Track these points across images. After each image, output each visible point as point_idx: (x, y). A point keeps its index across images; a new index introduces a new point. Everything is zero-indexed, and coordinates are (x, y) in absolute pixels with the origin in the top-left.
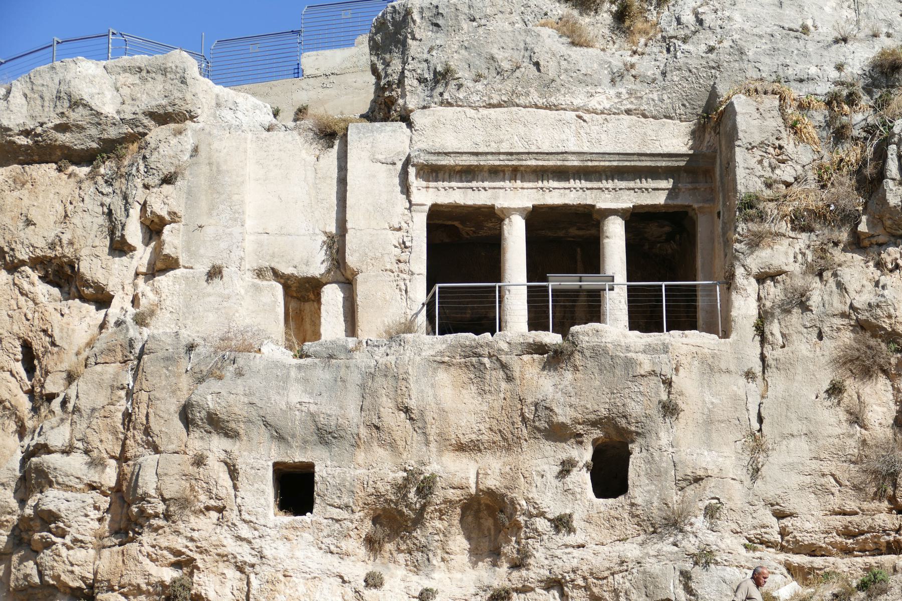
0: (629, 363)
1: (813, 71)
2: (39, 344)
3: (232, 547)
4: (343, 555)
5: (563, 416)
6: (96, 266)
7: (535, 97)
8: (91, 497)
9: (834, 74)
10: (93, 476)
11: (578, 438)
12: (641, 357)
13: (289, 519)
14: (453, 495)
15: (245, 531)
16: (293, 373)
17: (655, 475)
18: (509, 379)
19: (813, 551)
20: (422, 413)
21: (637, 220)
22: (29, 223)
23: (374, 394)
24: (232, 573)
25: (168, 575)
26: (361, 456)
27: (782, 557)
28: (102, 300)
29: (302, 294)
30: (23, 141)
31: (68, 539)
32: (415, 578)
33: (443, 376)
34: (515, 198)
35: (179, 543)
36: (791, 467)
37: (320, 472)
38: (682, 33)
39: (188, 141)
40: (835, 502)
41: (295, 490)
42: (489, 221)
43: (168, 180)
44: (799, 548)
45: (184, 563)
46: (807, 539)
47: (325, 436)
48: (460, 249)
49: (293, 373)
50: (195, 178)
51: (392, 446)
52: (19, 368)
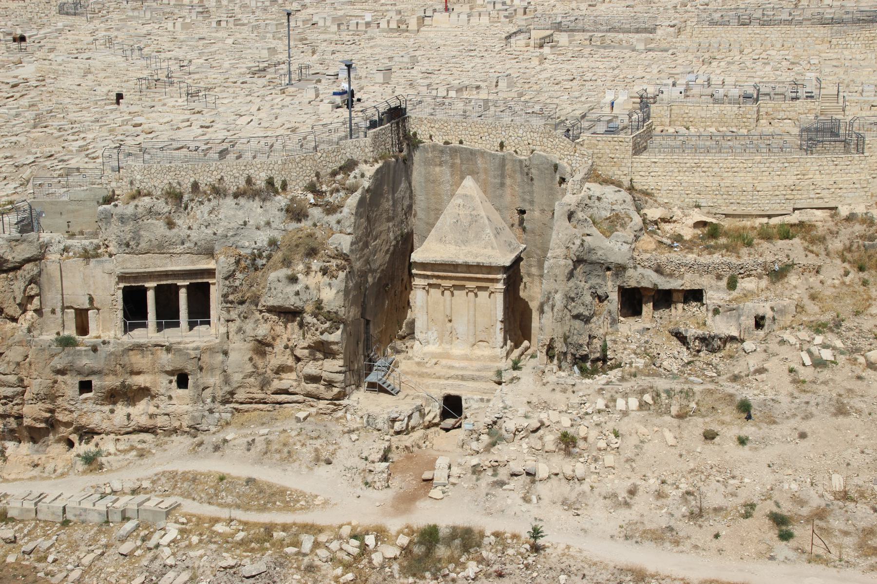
0: (188, 354)
3: (69, 407)
4: (102, 405)
5: (169, 368)
7: (157, 251)
8: (20, 389)
9: (254, 246)
11: (173, 375)
12: (192, 352)
13: (85, 396)
14: (135, 388)
17: (196, 386)
19: (242, 403)
23: (110, 360)
25: (48, 415)
26: (107, 378)
27: (232, 405)
28: (14, 320)
32: (124, 408)
33: (131, 353)
35: (51, 406)
40: (248, 390)
41: (85, 387)
44: (237, 402)
45: (52, 411)
47: (93, 373)
50: (43, 279)
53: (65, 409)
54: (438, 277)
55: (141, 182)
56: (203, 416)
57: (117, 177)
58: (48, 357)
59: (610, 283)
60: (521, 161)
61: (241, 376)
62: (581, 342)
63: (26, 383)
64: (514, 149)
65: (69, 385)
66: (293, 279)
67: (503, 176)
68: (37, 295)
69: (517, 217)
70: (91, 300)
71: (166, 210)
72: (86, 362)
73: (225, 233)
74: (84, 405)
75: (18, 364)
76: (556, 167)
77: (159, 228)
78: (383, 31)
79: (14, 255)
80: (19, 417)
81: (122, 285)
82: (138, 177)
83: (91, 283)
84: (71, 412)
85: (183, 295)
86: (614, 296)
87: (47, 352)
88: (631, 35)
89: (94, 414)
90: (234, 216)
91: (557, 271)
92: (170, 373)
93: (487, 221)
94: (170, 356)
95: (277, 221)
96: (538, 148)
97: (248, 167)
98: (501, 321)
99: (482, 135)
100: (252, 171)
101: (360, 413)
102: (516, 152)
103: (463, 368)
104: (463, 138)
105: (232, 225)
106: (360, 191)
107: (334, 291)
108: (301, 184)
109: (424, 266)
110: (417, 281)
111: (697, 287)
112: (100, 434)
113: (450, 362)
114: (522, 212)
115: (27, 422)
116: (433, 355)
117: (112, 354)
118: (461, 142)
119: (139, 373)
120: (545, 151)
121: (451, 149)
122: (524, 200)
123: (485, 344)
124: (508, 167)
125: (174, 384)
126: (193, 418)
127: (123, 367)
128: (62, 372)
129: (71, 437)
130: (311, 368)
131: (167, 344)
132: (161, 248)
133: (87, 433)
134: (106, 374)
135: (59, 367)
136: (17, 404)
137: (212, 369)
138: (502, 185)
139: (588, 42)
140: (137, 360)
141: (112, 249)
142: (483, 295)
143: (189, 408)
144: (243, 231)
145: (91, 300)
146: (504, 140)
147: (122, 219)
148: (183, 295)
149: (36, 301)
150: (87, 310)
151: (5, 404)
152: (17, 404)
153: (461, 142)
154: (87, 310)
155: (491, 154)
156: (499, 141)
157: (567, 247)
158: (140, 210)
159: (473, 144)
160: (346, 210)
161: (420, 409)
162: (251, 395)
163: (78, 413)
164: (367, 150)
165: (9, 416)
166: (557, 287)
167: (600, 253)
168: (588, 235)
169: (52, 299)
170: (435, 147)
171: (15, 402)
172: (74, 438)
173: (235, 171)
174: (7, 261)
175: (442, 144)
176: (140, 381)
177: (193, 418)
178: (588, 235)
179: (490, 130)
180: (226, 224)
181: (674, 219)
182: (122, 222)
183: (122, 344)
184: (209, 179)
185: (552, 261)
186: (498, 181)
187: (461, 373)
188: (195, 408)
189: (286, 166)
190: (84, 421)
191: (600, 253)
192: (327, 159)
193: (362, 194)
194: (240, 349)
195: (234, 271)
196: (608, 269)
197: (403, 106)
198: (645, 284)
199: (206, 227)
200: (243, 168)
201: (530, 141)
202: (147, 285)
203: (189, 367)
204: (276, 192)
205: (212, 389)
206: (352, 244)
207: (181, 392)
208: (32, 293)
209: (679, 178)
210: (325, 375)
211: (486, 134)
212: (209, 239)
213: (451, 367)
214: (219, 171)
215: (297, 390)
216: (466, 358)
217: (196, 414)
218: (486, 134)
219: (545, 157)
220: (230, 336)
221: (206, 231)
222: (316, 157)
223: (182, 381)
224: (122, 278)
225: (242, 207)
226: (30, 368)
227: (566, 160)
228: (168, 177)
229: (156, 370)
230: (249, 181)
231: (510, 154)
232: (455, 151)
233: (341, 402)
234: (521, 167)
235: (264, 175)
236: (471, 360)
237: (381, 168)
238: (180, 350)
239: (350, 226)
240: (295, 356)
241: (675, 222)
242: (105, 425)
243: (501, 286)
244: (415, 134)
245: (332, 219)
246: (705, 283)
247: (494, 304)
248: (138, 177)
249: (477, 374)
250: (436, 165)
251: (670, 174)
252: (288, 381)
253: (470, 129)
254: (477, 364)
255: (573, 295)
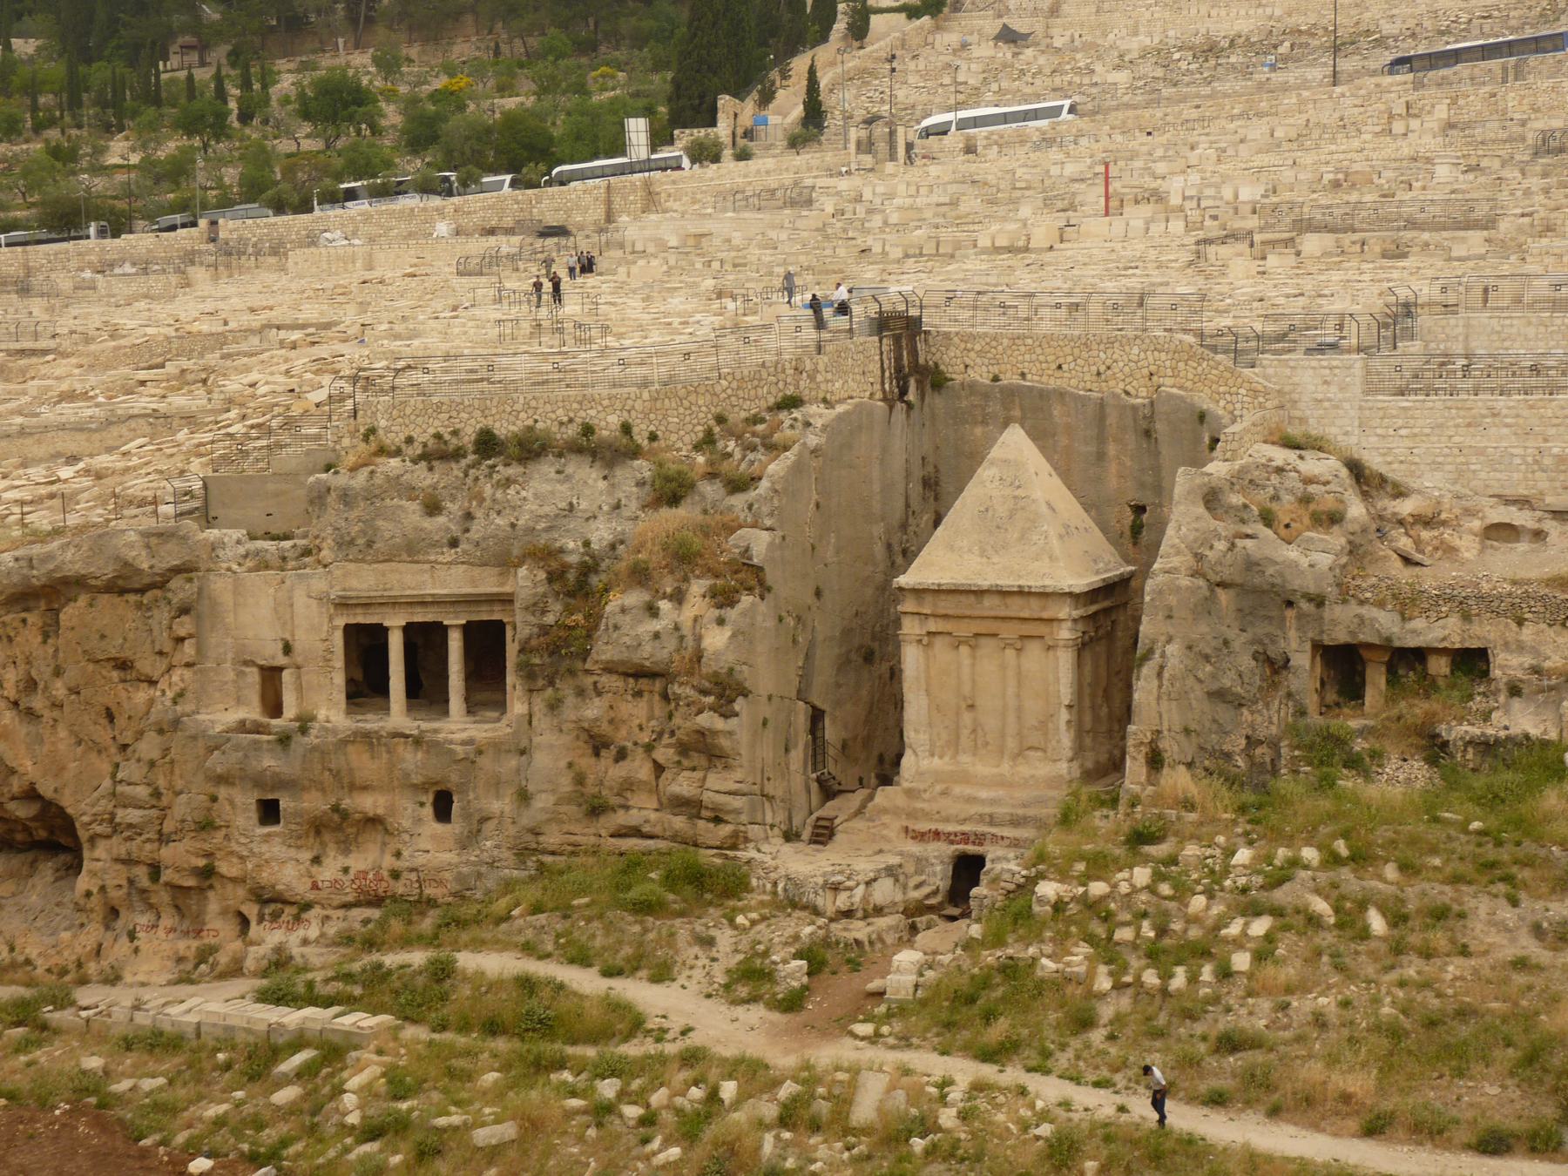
0: (451, 752)
1: (571, 545)
2: (114, 709)
3: (235, 847)
4: (299, 847)
5: (417, 779)
6: (146, 665)
8: (154, 813)
10: (154, 802)
12: (459, 748)
15: (243, 840)
16: (265, 746)
17: (467, 816)
18: (389, 752)
19: (553, 853)
20: (339, 772)
21: (469, 630)
22: (103, 637)
24: (235, 860)
25: (201, 862)
26: (306, 796)
28: (152, 683)
29: (271, 675)
30: (93, 582)
31: (143, 837)
33: (350, 748)
34: (395, 622)
35: (207, 846)
36: (543, 809)
37: (282, 804)
38: (497, 507)
39: (196, 583)
40: (566, 828)
41: (269, 812)
42: (380, 632)
43: (184, 610)
45: (209, 855)
46: (551, 848)
48: (365, 646)
49: (265, 746)
51: (323, 790)
52: (104, 722)
53: (232, 853)
54: (946, 616)
55: (388, 430)
56: (479, 875)
57: (352, 428)
58: (202, 752)
59: (1293, 634)
60: (1134, 408)
61: (552, 799)
62: (1226, 748)
63: (165, 801)
64: (1121, 385)
65: (240, 807)
66: (652, 611)
67: (1101, 439)
68: (191, 636)
69: (1129, 516)
70: (287, 649)
71: (428, 482)
72: (269, 762)
73: (531, 524)
74: (265, 848)
75: (152, 764)
76: (1202, 417)
77: (412, 513)
78: (984, 251)
79: (153, 561)
80: (155, 870)
81: (341, 622)
82: (383, 423)
83: (288, 617)
84: (241, 857)
85: (455, 643)
86: (1302, 659)
87: (201, 743)
88: (1445, 234)
89: (284, 863)
90: (552, 493)
91: (1172, 600)
92: (422, 788)
93: (1044, 509)
94: (420, 755)
95: (634, 505)
96: (1169, 381)
97: (586, 404)
98: (1069, 707)
99: (1061, 360)
100: (593, 413)
101: (773, 875)
102: (1127, 393)
103: (993, 802)
104: (1026, 368)
105: (547, 509)
106: (796, 448)
107: (727, 632)
108: (687, 439)
109: (919, 592)
110: (910, 627)
111: (1475, 644)
112: (294, 903)
113: (969, 791)
114: (1139, 509)
115: (167, 875)
116: (938, 777)
117: (315, 748)
118: (1023, 375)
119: (365, 788)
120: (1181, 388)
121: (1002, 390)
122: (1142, 485)
123: (1039, 754)
124: (1112, 419)
125: (428, 811)
126: (460, 878)
127: (336, 775)
128: (223, 779)
129: (245, 909)
130: (682, 785)
131: (415, 732)
132: (412, 550)
133: (272, 902)
134: (304, 789)
135: (219, 770)
136: (148, 840)
137: (496, 784)
138: (1101, 456)
139: (1357, 248)
140: (364, 764)
141: (326, 554)
142: (1034, 650)
143: (451, 857)
144: (565, 521)
145: (287, 649)
146: (1103, 368)
147: (346, 498)
148: (455, 643)
149: (189, 649)
150: (280, 669)
151: (130, 839)
152: (148, 840)
153: (1023, 375)
154: (280, 669)
155: (1076, 398)
156: (1094, 369)
157: (1196, 555)
158: (379, 480)
159: (1044, 379)
160: (765, 484)
161: (891, 871)
162: (573, 838)
163: (255, 860)
164: (819, 378)
165: (138, 863)
166: (1171, 631)
167: (1270, 570)
168: (1248, 536)
169: (220, 644)
170: (972, 387)
171: (143, 837)
172: (251, 910)
173: (560, 412)
174: (139, 572)
175: (988, 382)
176: (369, 803)
177: (460, 878)
178: (1248, 536)
179: (1076, 351)
180: (534, 507)
181: (1443, 516)
182: (346, 504)
183: (334, 731)
184: (515, 429)
185: (1160, 578)
186: (1092, 448)
187: (987, 810)
188: (464, 858)
189: (659, 405)
190: (265, 877)
191: (1270, 570)
192: (740, 393)
193: (800, 455)
194: (551, 746)
195: (545, 595)
196: (1290, 604)
197: (913, 312)
198: (1365, 636)
199: (499, 513)
200: (575, 406)
201: (1153, 368)
202: (386, 623)
203: (454, 779)
204: (635, 453)
205: (495, 821)
206: (771, 545)
207: (439, 828)
208: (182, 633)
209: (1457, 439)
210: (708, 797)
211: (1070, 358)
212: (501, 534)
213: (971, 800)
214: (530, 412)
215: (658, 830)
216: (1001, 782)
217: (465, 870)
218: (1070, 358)
219: (1181, 398)
220: (535, 723)
221: (499, 521)
222: (718, 389)
223: (443, 807)
224: (343, 604)
225: (568, 478)
226: (172, 772)
227: (1222, 403)
228: (437, 423)
229: (396, 783)
230: (588, 430)
231: (1115, 396)
232: (1011, 393)
233: (739, 854)
234: (1135, 420)
235: (614, 420)
236: (1011, 785)
237: (847, 413)
238: (437, 744)
239: (771, 514)
240: (655, 762)
241: (1444, 523)
242: (302, 889)
243: (1065, 633)
244: (936, 364)
245: (738, 501)
246: (1492, 636)
247: (1054, 673)
248: (383, 423)
249: (1020, 812)
250: (976, 423)
251: (1437, 431)
252: (644, 810)
253: (1039, 351)
254: (1021, 795)
255: (1208, 651)
